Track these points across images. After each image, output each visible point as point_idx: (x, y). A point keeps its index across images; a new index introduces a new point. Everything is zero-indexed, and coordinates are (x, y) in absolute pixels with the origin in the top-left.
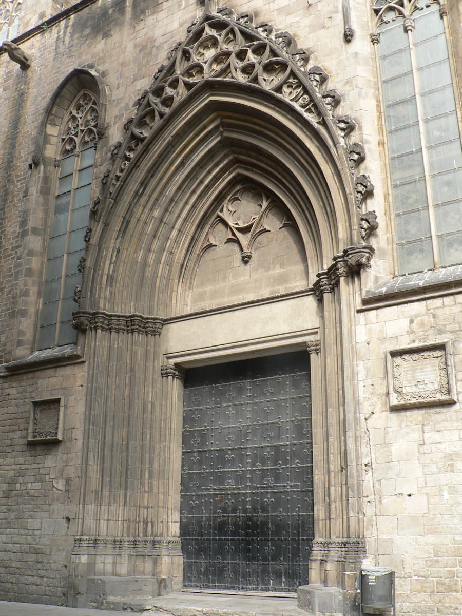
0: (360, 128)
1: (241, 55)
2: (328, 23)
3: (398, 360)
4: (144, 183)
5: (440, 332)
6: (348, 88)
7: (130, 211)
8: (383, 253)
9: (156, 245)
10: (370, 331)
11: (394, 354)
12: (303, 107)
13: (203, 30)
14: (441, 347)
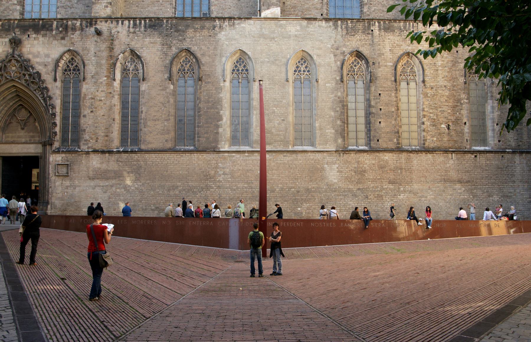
0: (56, 108)
1: (24, 75)
2: (50, 73)
3: (59, 166)
5: (68, 161)
6: (53, 96)
8: (58, 141)
10: (53, 159)
11: (58, 164)
12: (42, 98)
13: (12, 60)
14: (67, 165)
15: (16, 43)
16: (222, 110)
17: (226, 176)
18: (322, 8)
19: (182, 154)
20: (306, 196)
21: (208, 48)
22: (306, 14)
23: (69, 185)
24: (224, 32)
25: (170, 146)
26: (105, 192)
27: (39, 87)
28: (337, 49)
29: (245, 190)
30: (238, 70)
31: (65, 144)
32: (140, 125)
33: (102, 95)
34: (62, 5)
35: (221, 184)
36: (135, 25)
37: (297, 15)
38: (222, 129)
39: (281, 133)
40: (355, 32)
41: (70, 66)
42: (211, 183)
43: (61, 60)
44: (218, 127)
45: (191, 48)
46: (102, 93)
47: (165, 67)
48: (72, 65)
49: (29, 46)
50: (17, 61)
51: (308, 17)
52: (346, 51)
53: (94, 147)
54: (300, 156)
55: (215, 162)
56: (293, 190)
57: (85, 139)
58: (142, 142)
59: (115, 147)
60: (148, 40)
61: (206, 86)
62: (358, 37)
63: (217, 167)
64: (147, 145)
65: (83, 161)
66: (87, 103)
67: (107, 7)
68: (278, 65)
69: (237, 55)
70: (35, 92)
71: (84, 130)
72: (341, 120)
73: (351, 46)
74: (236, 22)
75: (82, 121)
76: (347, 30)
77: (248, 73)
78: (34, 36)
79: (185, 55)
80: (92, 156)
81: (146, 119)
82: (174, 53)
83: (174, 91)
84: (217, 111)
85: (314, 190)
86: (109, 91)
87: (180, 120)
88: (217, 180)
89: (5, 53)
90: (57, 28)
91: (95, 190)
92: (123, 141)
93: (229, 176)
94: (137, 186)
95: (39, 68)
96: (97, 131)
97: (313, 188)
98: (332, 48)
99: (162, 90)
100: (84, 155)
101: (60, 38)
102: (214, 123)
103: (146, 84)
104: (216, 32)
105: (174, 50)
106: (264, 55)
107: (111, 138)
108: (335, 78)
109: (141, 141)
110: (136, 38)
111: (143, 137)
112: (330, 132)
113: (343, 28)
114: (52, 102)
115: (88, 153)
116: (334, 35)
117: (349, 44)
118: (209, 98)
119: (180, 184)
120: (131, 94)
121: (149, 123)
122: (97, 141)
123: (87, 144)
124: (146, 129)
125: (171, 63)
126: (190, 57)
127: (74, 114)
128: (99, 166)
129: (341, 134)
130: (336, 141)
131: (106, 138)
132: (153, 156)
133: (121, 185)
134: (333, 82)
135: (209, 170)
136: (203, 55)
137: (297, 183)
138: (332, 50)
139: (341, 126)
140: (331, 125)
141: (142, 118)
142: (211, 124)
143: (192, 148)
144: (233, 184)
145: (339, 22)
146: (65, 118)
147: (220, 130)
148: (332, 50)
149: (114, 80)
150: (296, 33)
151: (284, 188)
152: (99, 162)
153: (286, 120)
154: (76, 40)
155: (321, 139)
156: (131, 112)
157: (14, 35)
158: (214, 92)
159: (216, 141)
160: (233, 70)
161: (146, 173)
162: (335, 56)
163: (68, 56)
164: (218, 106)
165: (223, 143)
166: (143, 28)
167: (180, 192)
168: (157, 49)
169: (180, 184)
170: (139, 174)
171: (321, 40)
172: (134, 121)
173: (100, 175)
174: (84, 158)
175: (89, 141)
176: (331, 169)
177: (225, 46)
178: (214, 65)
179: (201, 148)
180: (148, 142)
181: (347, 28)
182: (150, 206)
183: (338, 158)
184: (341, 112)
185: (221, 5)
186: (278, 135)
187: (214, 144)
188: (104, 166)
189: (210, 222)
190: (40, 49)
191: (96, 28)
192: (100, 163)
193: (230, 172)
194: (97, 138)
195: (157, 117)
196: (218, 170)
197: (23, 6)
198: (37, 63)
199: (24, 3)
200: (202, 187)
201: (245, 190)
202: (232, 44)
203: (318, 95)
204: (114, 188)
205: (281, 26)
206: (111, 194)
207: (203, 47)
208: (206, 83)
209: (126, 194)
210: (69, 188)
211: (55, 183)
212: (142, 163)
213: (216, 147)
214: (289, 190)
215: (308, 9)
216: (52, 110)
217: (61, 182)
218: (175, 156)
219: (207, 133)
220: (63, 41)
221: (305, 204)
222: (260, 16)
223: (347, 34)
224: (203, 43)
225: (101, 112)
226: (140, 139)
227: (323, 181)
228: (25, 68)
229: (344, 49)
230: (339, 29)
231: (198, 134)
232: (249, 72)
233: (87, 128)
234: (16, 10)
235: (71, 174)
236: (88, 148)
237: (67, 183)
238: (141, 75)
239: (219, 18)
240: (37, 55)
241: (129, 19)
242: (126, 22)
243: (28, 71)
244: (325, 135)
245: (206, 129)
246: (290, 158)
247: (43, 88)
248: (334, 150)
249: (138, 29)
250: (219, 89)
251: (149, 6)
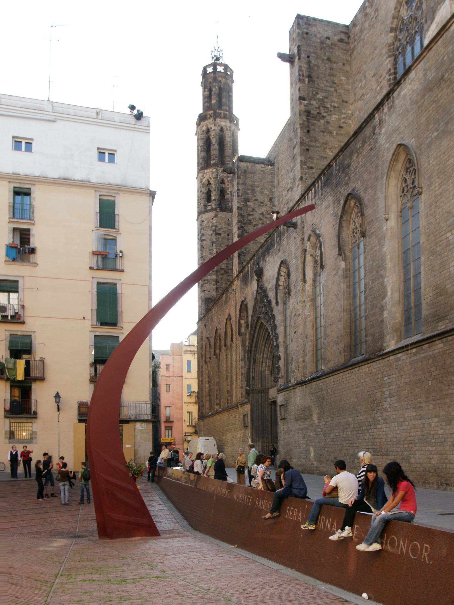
4: (256, 347)
7: (255, 356)
8: (282, 377)
9: (264, 365)
25: (343, 360)
43: (280, 277)
59: (309, 375)
84: (381, 280)
86: (303, 300)
93: (396, 398)
102: (379, 305)
118: (373, 261)
122: (299, 370)
131: (303, 364)
135: (376, 391)
165: (389, 336)
196: (384, 389)
216: (276, 341)
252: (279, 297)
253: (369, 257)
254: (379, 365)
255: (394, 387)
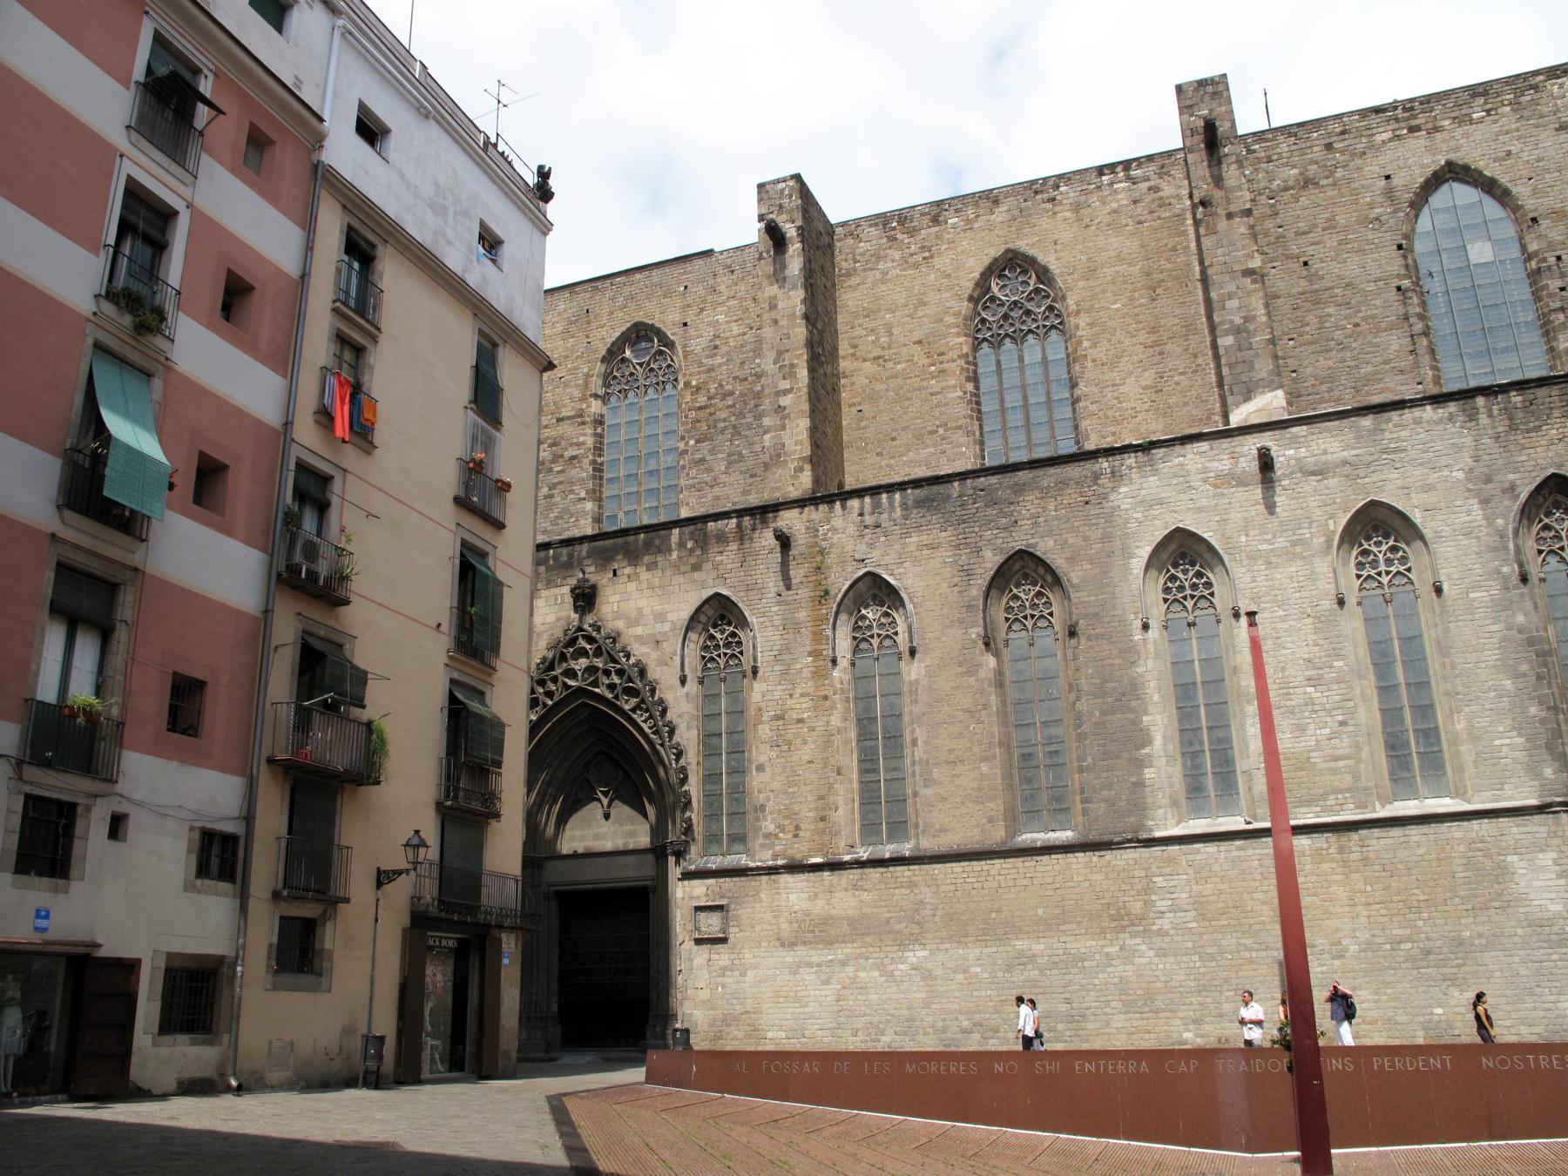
5: (723, 897)
11: (698, 909)
13: (577, 638)
15: (585, 598)
16: (1146, 712)
17: (1182, 914)
18: (1416, 365)
19: (1039, 858)
20: (1459, 966)
21: (1086, 538)
22: (1368, 394)
23: (728, 963)
24: (1126, 485)
25: (1003, 833)
26: (826, 982)
27: (643, 701)
28: (1488, 480)
29: (1247, 955)
30: (1181, 588)
31: (715, 848)
32: (909, 780)
33: (804, 706)
34: (691, 482)
35: (1166, 939)
36: (876, 506)
37: (1339, 400)
38: (1152, 770)
39: (1341, 764)
40: (1538, 419)
41: (718, 636)
42: (1138, 940)
44: (1139, 764)
45: (1034, 546)
46: (802, 700)
47: (969, 607)
48: (722, 632)
49: (617, 597)
50: (590, 640)
51: (1376, 399)
52: (1518, 482)
53: (789, 852)
54: (1413, 832)
55: (1143, 873)
56: (1409, 945)
57: (764, 831)
58: (921, 829)
60: (913, 539)
61: (1091, 647)
62: (1554, 431)
63: (1148, 889)
64: (934, 836)
65: (762, 895)
66: (765, 730)
67: (801, 469)
68: (1303, 558)
69: (1173, 546)
70: (635, 716)
71: (763, 807)
72: (1541, 703)
73: (1533, 463)
74: (1159, 453)
75: (757, 782)
76: (1511, 419)
77: (1212, 594)
78: (627, 570)
79: (1023, 568)
80: (785, 879)
81: (927, 762)
82: (989, 565)
83: (999, 673)
84: (1132, 716)
85: (1484, 942)
86: (822, 693)
87: (1023, 755)
88: (1154, 928)
89: (563, 622)
90: (682, 545)
91: (798, 977)
92: (869, 830)
94: (915, 960)
95: (640, 651)
96: (796, 808)
97: (1480, 936)
98: (1469, 480)
99: (969, 673)
100: (765, 878)
101: (688, 568)
103: (920, 661)
104: (1101, 490)
105: (991, 560)
106: (1252, 533)
107: (835, 823)
108: (1499, 572)
109: (917, 825)
110: (883, 539)
111: (922, 814)
112: (1509, 744)
113: (1496, 412)
114: (676, 738)
115: (773, 871)
116: (1469, 441)
117: (1524, 458)
119: (1042, 947)
120: (882, 696)
121: (936, 773)
122: (796, 836)
123: (771, 846)
124: (929, 792)
125: (987, 595)
126: (1035, 571)
127: (733, 763)
128: (806, 905)
129: (1549, 748)
130: (1533, 771)
131: (821, 825)
132: (957, 867)
133: (867, 959)
134: (1490, 583)
135: (1127, 899)
136: (1073, 560)
137: (1420, 923)
138: (1470, 486)
139: (1543, 721)
140: (1508, 722)
141: (917, 758)
142: (1118, 757)
143: (1065, 836)
144: (1205, 937)
145: (1480, 401)
146: (711, 777)
147: (1149, 773)
148: (1470, 486)
149: (834, 662)
150: (1346, 453)
151: (1378, 940)
152: (805, 895)
153: (1351, 722)
154: (729, 566)
155: (1482, 768)
156: (885, 746)
157: (581, 575)
158: (1117, 661)
159: (1140, 807)
160: (1167, 590)
161: (937, 919)
162: (1484, 502)
163: (710, 612)
164: (1133, 703)
165: (1161, 811)
166: (898, 509)
167: (1042, 972)
168: (941, 560)
169: (1042, 947)
170: (918, 923)
171: (1430, 461)
172: (895, 770)
173: (809, 932)
174: (764, 886)
175: (776, 836)
176: (1535, 869)
177: (1133, 525)
178: (1108, 585)
179: (1093, 833)
180: (937, 826)
181: (1508, 412)
182: (957, 1019)
183: (1553, 829)
184: (1539, 677)
185: (1109, 413)
186: (1335, 771)
187: (1132, 819)
188: (820, 906)
189: (1139, 1064)
190: (643, 603)
191: (775, 530)
192: (810, 898)
193: (1192, 900)
194: (797, 828)
195: (958, 753)
196: (1154, 897)
197: (600, 499)
198: (637, 638)
199: (601, 492)
200: (1108, 954)
201: (1247, 955)
202: (1154, 518)
203: (1447, 630)
204: (850, 969)
205: (1293, 442)
206: (844, 988)
207: (1071, 539)
208: (1089, 639)
209: (885, 985)
210: (728, 973)
211: (691, 960)
212: (924, 889)
213: (1141, 827)
214: (1392, 949)
215: (1369, 380)
216: (677, 760)
217: (706, 956)
218: (1021, 865)
219: (1109, 787)
220: (696, 575)
221: (1456, 994)
222: (1227, 422)
223: (1513, 427)
224: (1068, 525)
225: (806, 752)
226: (912, 819)
227: (1509, 910)
228: (610, 655)
229: (1511, 477)
230: (1483, 419)
231: (1082, 792)
232: (1215, 589)
233: (769, 800)
234: (584, 513)
235: (734, 934)
236: (775, 857)
237: (722, 956)
238: (902, 638)
239: (1110, 452)
240: (633, 622)
241: (859, 493)
242: (854, 503)
243: (617, 662)
244: (1491, 758)
245: (1104, 775)
246: (1382, 841)
247: (654, 703)
248: (1534, 802)
249: (885, 516)
250: (1130, 654)
251: (909, 450)
252: (686, 664)
253: (1090, 671)
254: (1137, 855)
255: (1186, 895)
